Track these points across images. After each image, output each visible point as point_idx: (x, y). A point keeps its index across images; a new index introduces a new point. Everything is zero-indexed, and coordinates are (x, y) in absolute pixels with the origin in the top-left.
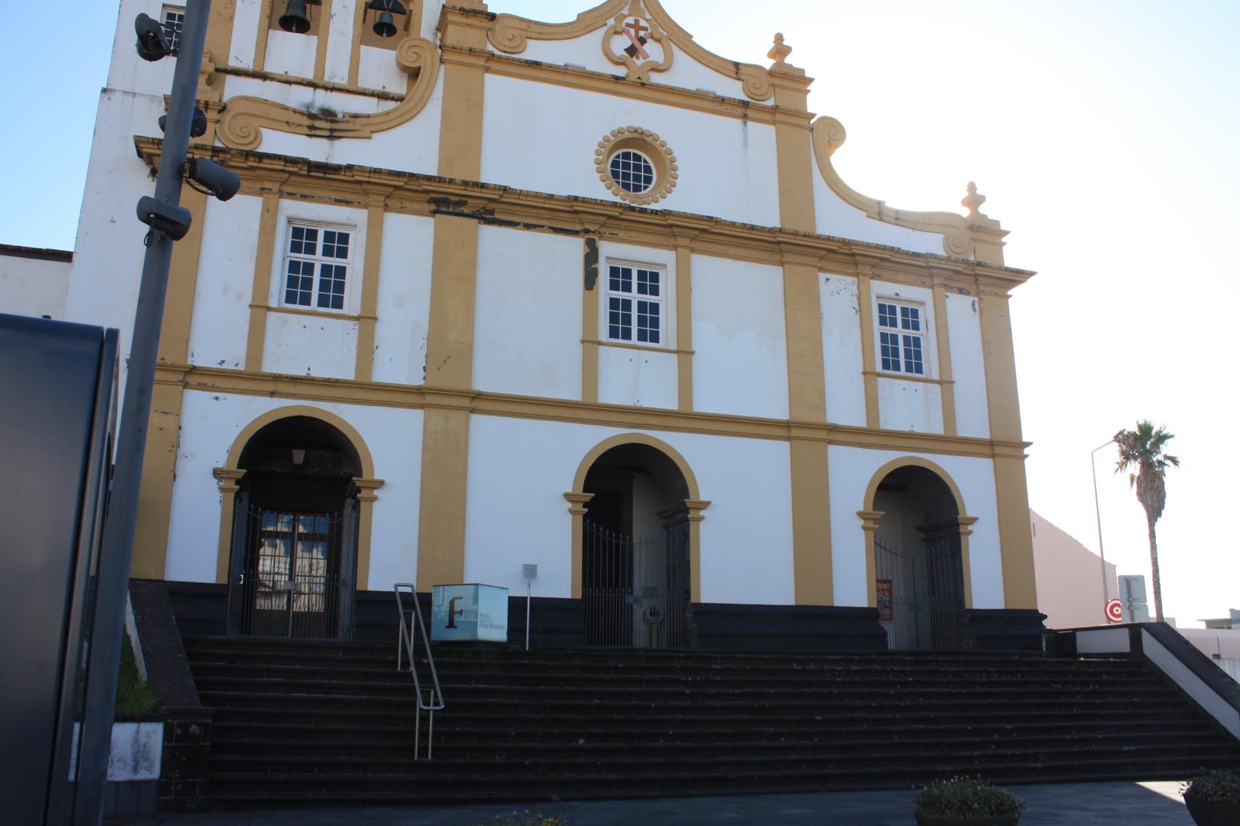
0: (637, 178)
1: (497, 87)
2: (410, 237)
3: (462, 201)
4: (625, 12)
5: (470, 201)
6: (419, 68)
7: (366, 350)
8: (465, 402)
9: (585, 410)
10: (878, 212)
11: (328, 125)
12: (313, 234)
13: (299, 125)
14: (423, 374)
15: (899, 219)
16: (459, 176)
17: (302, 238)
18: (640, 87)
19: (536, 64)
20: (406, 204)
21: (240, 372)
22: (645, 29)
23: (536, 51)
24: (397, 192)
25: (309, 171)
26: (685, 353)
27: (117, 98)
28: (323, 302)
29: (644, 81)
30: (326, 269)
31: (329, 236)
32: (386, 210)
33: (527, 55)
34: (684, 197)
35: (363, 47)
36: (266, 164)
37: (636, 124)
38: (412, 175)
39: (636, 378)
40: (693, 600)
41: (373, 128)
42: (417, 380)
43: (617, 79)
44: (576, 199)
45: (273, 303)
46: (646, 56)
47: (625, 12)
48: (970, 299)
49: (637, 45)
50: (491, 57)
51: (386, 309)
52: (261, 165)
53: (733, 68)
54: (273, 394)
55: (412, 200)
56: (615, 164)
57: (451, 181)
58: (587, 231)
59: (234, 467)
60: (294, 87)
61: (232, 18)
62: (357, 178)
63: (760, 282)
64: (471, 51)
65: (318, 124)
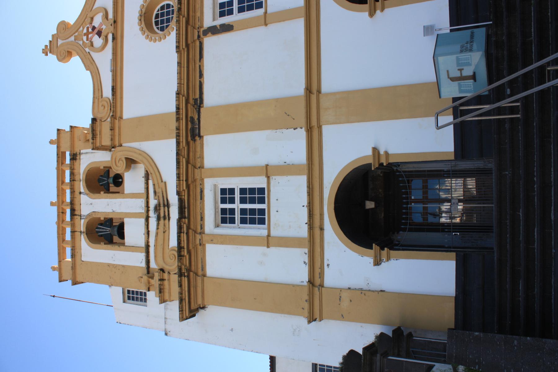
1: (130, 110)
2: (219, 150)
3: (190, 121)
4: (81, 42)
5: (189, 115)
6: (127, 159)
7: (287, 169)
8: (314, 97)
11: (162, 208)
12: (224, 211)
13: (164, 225)
14: (299, 129)
16: (174, 124)
17: (227, 217)
18: (117, 22)
19: (114, 89)
20: (198, 155)
21: (310, 252)
22: (88, 28)
24: (191, 162)
25: (185, 218)
27: (169, 328)
28: (262, 201)
30: (243, 201)
31: (223, 201)
32: (203, 167)
33: (110, 96)
35: (126, 192)
36: (184, 244)
37: (137, 21)
38: (178, 154)
41: (160, 181)
42: (302, 133)
43: (114, 39)
44: (178, 47)
45: (265, 233)
46: (101, 24)
47: (81, 42)
49: (96, 31)
51: (260, 160)
52: (185, 247)
54: (322, 229)
55: (195, 152)
57: (178, 129)
58: (199, 37)
59: (371, 252)
60: (150, 229)
61: (123, 266)
62: (185, 188)
64: (112, 129)
65: (162, 215)
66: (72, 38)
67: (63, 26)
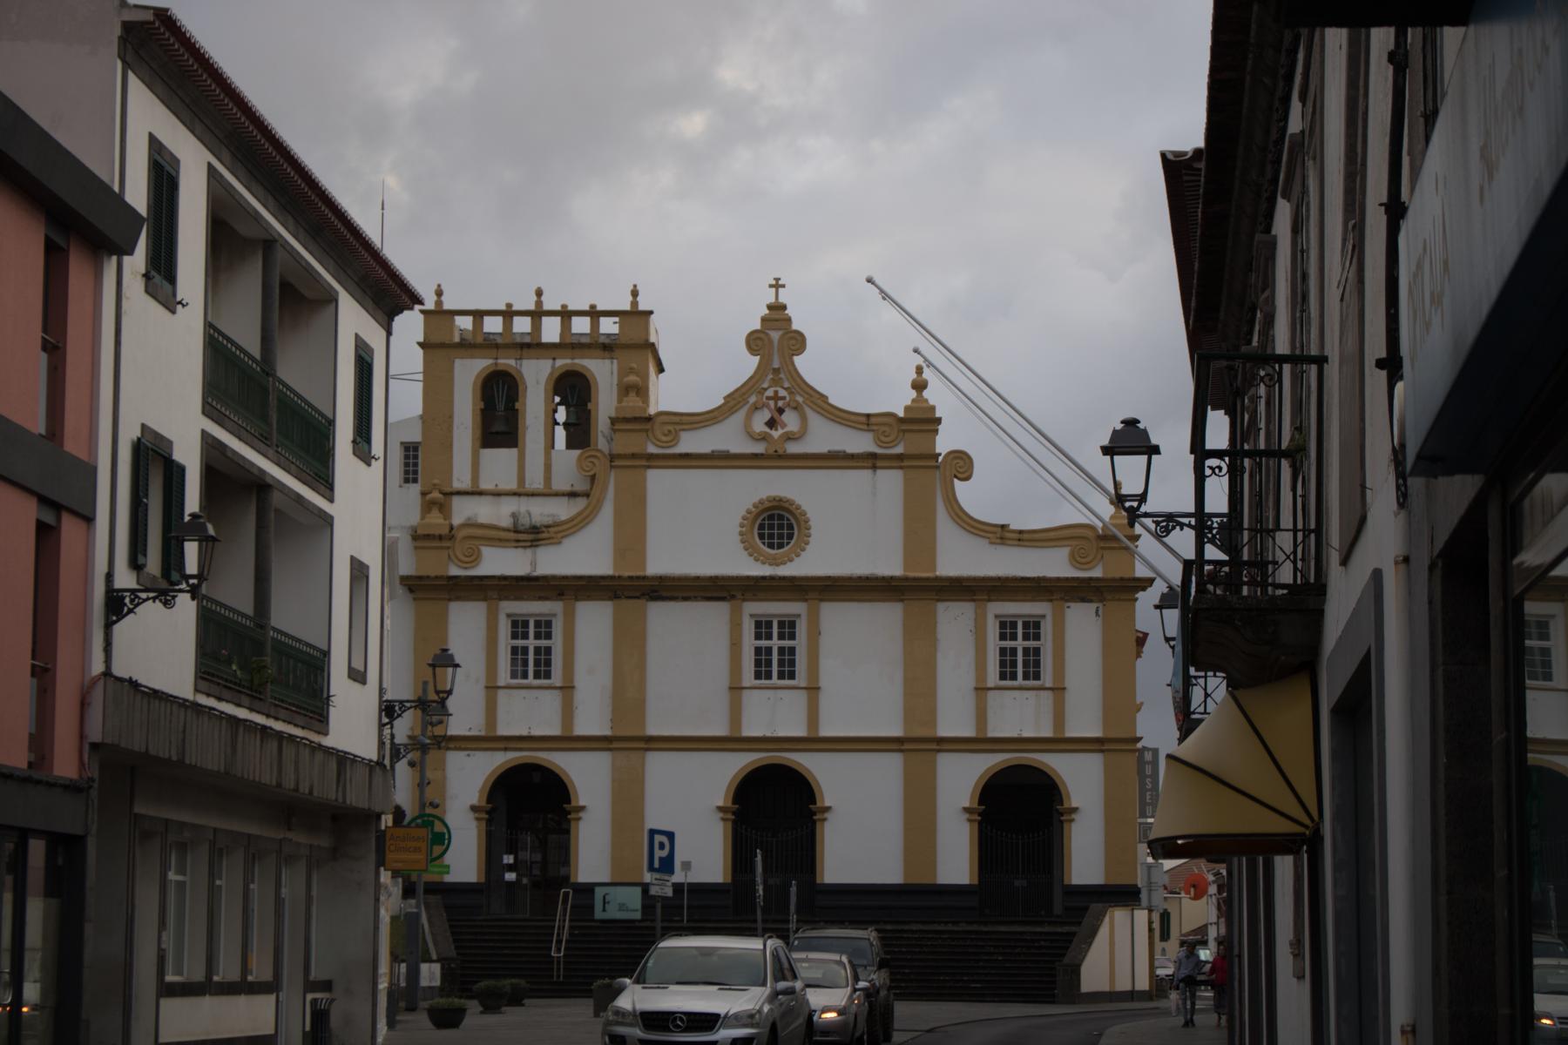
0: (781, 536)
1: (659, 482)
4: (765, 385)
8: (642, 745)
9: (732, 742)
10: (1001, 535)
15: (1025, 539)
22: (783, 398)
23: (691, 443)
26: (813, 690)
29: (780, 452)
30: (537, 650)
31: (538, 624)
33: (682, 448)
34: (808, 564)
39: (774, 714)
40: (818, 881)
43: (755, 456)
46: (784, 425)
48: (1093, 606)
49: (776, 415)
50: (651, 457)
51: (581, 680)
53: (864, 419)
54: (506, 749)
56: (761, 527)
60: (504, 499)
63: (886, 618)
64: (634, 456)
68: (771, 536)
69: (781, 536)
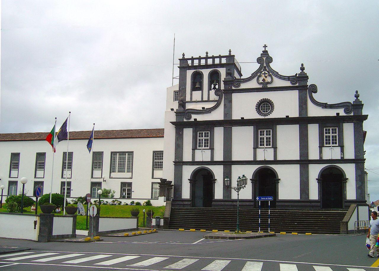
3: (228, 124)
10: (325, 106)
15: (332, 106)
18: (265, 88)
23: (243, 86)
33: (240, 88)
39: (265, 154)
47: (262, 71)
49: (265, 78)
63: (295, 129)
66: (265, 65)
67: (270, 60)
68: (264, 109)
69: (267, 109)
